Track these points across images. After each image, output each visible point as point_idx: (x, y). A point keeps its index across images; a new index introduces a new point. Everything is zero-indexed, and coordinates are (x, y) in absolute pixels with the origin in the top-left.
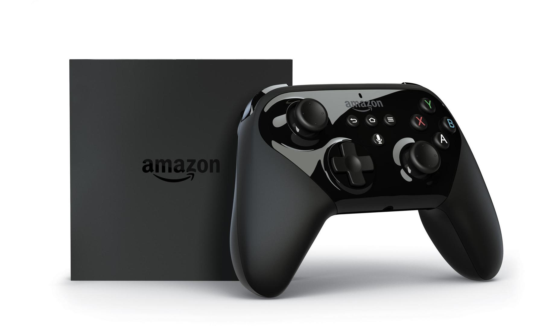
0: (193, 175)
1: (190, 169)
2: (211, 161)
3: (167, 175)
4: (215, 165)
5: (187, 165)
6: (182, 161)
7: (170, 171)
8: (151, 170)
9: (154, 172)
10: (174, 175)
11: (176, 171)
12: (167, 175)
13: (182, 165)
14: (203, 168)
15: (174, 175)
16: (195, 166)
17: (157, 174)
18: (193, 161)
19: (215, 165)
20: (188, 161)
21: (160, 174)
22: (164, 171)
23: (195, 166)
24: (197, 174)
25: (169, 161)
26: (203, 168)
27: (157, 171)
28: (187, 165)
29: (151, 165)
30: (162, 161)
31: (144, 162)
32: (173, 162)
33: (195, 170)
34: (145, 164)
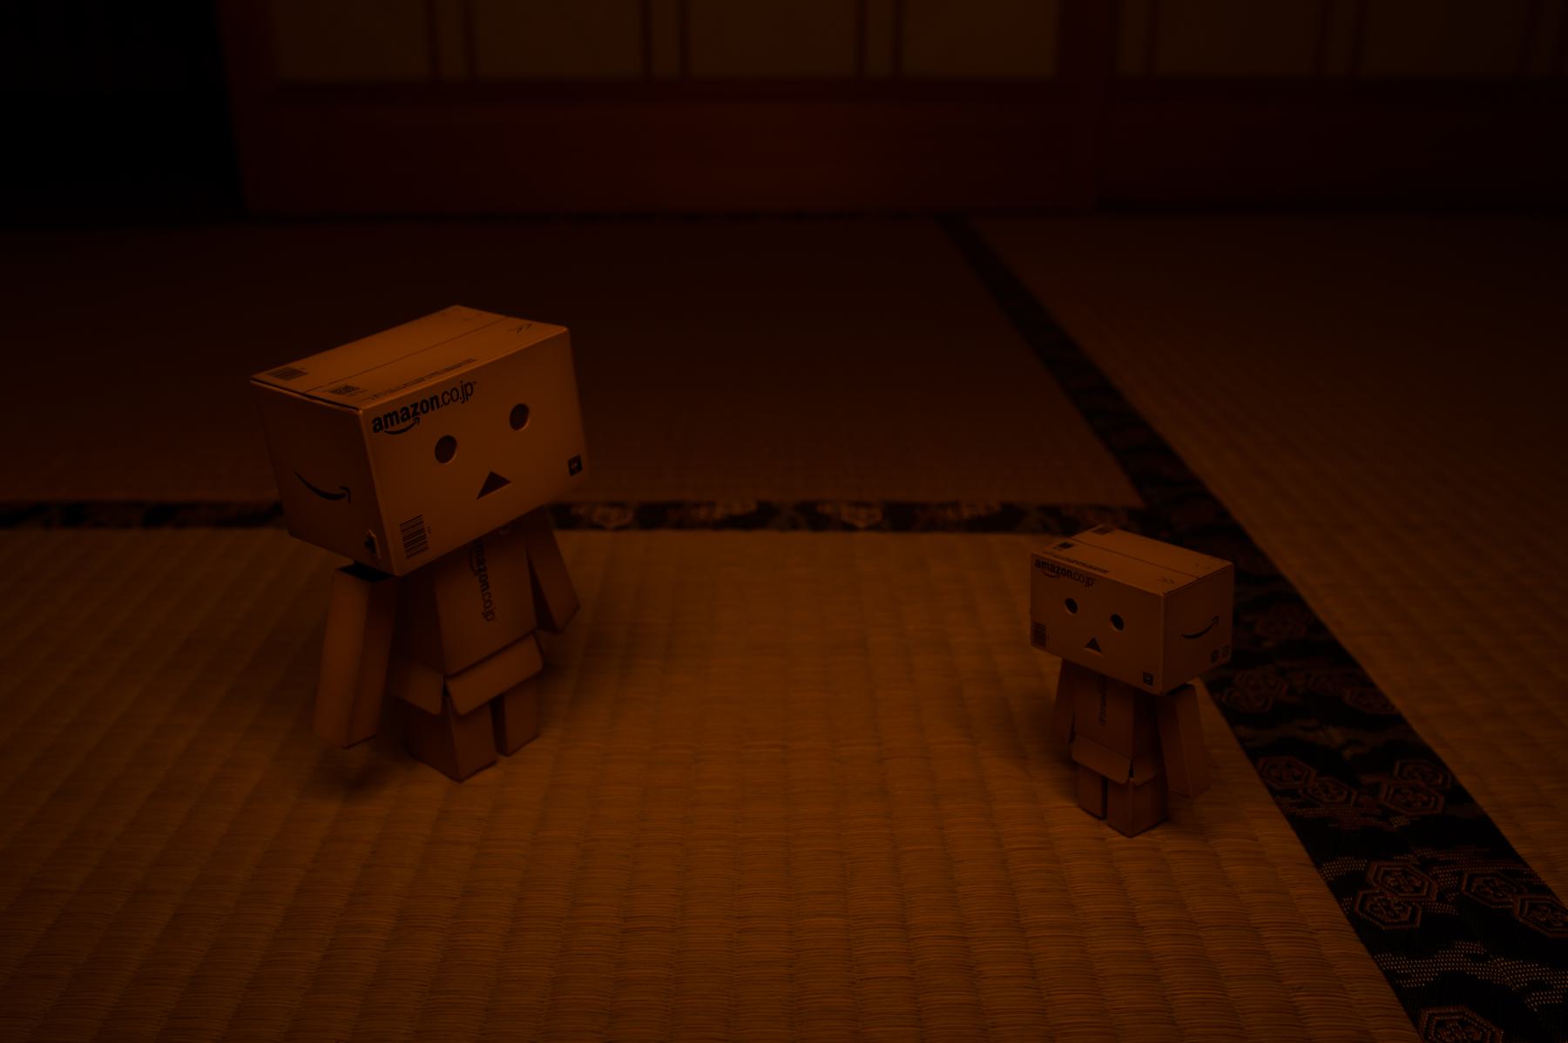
0: (418, 419)
1: (415, 413)
2: (432, 399)
3: (396, 428)
4: (435, 402)
5: (411, 410)
6: (406, 409)
7: (398, 422)
8: (381, 428)
9: (385, 429)
10: (403, 425)
11: (404, 420)
12: (396, 428)
13: (407, 413)
14: (425, 408)
15: (403, 425)
16: (419, 410)
17: (388, 430)
18: (415, 406)
19: (435, 402)
20: (412, 406)
21: (391, 429)
22: (393, 424)
23: (419, 410)
24: (422, 416)
25: (395, 413)
26: (425, 408)
27: (387, 427)
28: (411, 410)
29: (380, 423)
30: (390, 415)
31: (374, 422)
32: (399, 411)
33: (418, 414)
34: (373, 425)
